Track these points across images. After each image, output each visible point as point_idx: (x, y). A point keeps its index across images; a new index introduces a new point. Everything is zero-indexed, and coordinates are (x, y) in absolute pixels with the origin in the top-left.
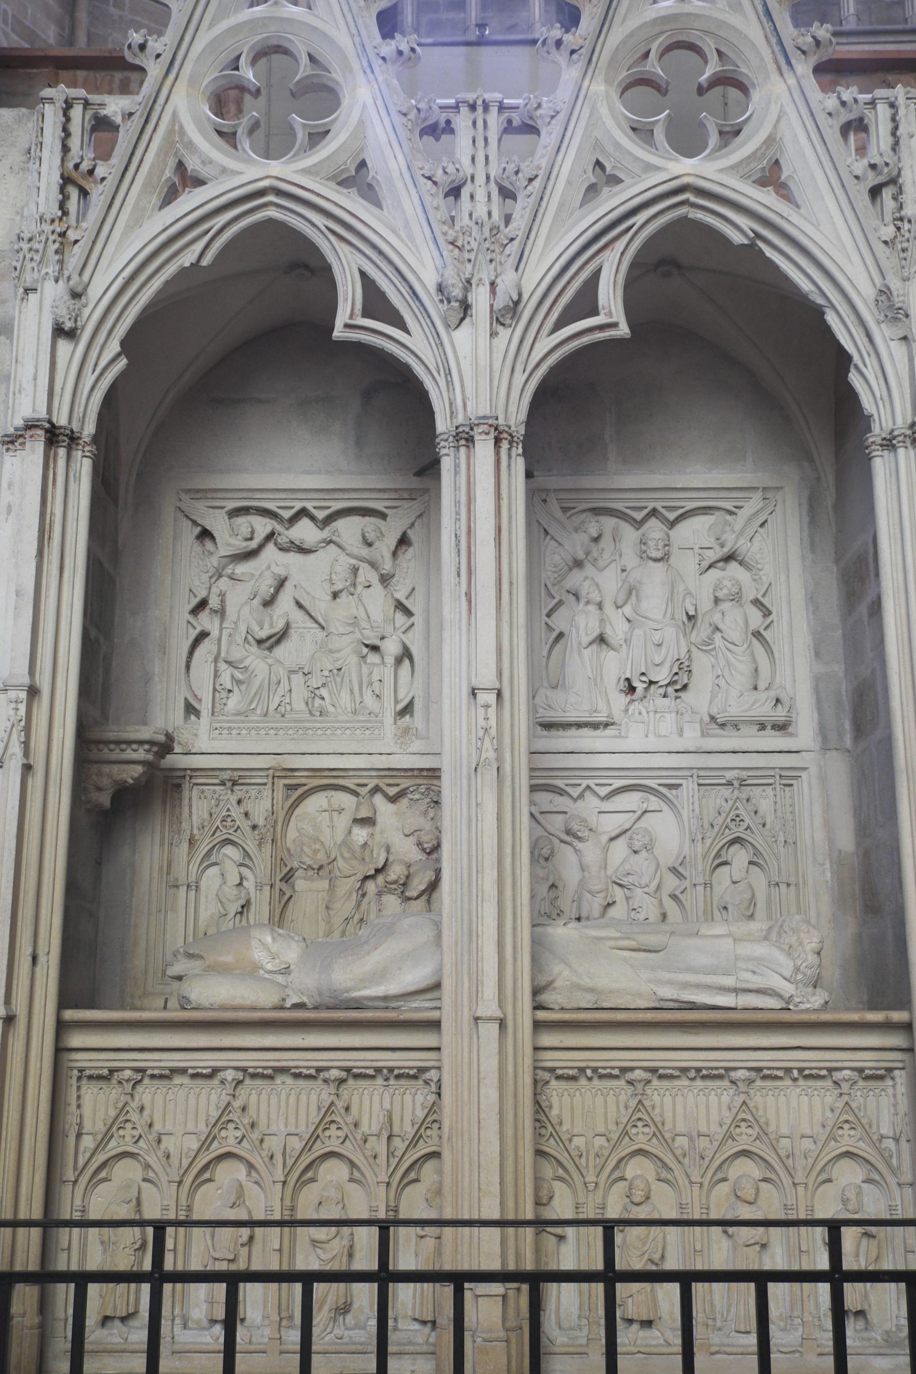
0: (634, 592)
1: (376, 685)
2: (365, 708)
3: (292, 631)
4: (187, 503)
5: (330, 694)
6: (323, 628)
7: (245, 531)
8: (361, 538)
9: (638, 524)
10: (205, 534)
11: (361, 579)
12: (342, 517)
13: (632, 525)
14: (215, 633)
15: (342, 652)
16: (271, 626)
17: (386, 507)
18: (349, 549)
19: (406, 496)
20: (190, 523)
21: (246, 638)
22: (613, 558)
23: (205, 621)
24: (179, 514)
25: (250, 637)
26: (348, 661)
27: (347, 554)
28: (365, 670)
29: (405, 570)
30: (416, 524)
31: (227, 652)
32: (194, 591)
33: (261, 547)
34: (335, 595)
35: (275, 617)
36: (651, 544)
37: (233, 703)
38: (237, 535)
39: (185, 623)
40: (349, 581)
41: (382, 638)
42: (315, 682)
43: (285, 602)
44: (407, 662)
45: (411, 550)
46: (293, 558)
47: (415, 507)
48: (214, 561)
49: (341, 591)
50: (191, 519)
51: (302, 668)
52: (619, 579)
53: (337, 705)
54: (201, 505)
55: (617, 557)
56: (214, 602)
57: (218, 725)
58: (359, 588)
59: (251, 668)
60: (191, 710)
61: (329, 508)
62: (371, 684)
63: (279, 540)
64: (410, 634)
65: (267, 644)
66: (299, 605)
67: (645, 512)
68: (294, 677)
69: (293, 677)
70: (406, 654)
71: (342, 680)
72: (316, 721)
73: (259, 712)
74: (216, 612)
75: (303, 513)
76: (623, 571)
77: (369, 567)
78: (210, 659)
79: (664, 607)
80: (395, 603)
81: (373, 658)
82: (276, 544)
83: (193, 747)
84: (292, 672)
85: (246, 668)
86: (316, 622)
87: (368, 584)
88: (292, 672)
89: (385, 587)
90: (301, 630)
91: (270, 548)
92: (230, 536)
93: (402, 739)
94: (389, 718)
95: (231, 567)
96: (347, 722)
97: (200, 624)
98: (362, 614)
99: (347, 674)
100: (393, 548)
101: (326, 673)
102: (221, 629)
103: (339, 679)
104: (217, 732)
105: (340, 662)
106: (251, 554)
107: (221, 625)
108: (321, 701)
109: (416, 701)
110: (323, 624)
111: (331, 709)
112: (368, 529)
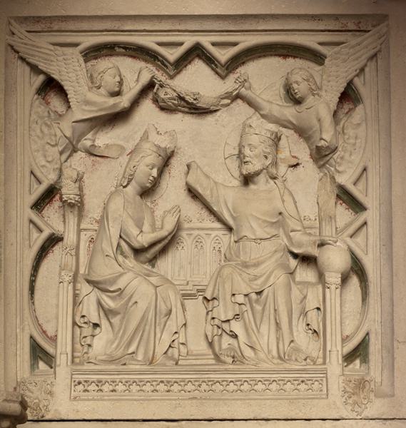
1: (313, 317)
2: (297, 350)
3: (184, 234)
4: (23, 39)
5: (247, 330)
6: (230, 229)
7: (110, 81)
8: (282, 91)
10: (51, 86)
11: (284, 154)
12: (252, 59)
14: (70, 238)
15: (263, 266)
16: (154, 229)
17: (321, 44)
18: (267, 108)
19: (351, 26)
20: (27, 69)
21: (119, 245)
23: (53, 218)
24: (12, 55)
26: (271, 281)
27: (263, 116)
28: (296, 293)
29: (352, 141)
30: (367, 69)
32: (38, 174)
33: (135, 103)
34: (247, 180)
35: (159, 213)
37: (101, 343)
38: (99, 87)
39: (26, 222)
40: (270, 158)
41: (321, 245)
42: (222, 312)
43: (172, 190)
44: (354, 281)
45: (360, 109)
46: (181, 123)
47: (367, 43)
48: (67, 127)
49: (257, 174)
50: (28, 64)
51: (203, 291)
53: (258, 347)
54: (43, 41)
56: (69, 191)
57: (81, 378)
58: (282, 169)
59: (128, 292)
60: (39, 353)
61: (235, 44)
62: (304, 313)
63: (162, 95)
64: (360, 239)
65: (149, 255)
66: (193, 193)
69: (188, 303)
70: (357, 269)
71: (263, 310)
72: (227, 371)
73: (140, 357)
74: (72, 206)
75: (197, 52)
77: (296, 136)
78: (67, 279)
80: (336, 191)
81: (306, 274)
82: (156, 101)
83: (47, 411)
84: (186, 296)
85: (120, 291)
86: (219, 219)
87: (294, 162)
88: (186, 296)
89: (320, 167)
90: (196, 232)
91: (147, 106)
92: (90, 89)
93: (354, 398)
94: (335, 365)
95: (89, 136)
96: (278, 372)
97: (48, 225)
98: (290, 207)
99: (270, 300)
100: (333, 106)
101: (240, 299)
102: (79, 231)
103: (258, 308)
104: (80, 387)
105: (259, 282)
106: (117, 118)
107: (79, 225)
108: (232, 341)
109: (372, 337)
110: (231, 222)
111: (248, 352)
112: (296, 77)
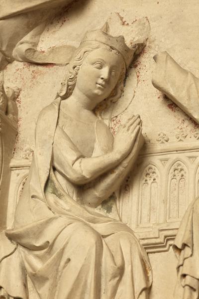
3: (155, 160)
25: (60, 181)
31: (16, 222)
43: (140, 100)
51: (172, 237)
65: (99, 192)
66: (171, 102)
68: (156, 260)
88: (150, 248)
90: (173, 156)
95: (27, 38)
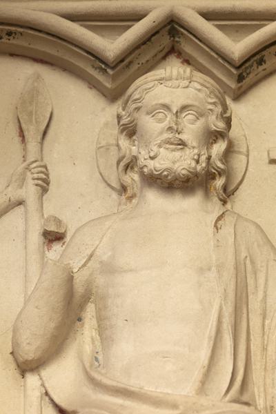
0: (90, 311)
9: (115, 76)
13: (93, 84)
22: (14, 193)
36: (152, 126)
52: (34, 268)
55: (30, 191)
67: (137, 30)
76: (53, 237)
79: (204, 354)
